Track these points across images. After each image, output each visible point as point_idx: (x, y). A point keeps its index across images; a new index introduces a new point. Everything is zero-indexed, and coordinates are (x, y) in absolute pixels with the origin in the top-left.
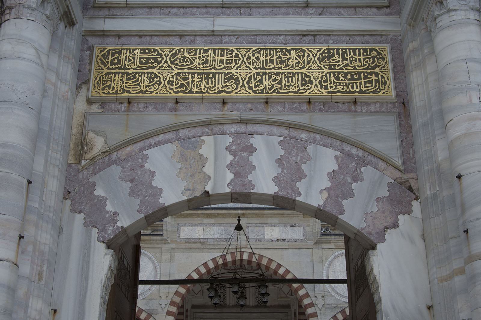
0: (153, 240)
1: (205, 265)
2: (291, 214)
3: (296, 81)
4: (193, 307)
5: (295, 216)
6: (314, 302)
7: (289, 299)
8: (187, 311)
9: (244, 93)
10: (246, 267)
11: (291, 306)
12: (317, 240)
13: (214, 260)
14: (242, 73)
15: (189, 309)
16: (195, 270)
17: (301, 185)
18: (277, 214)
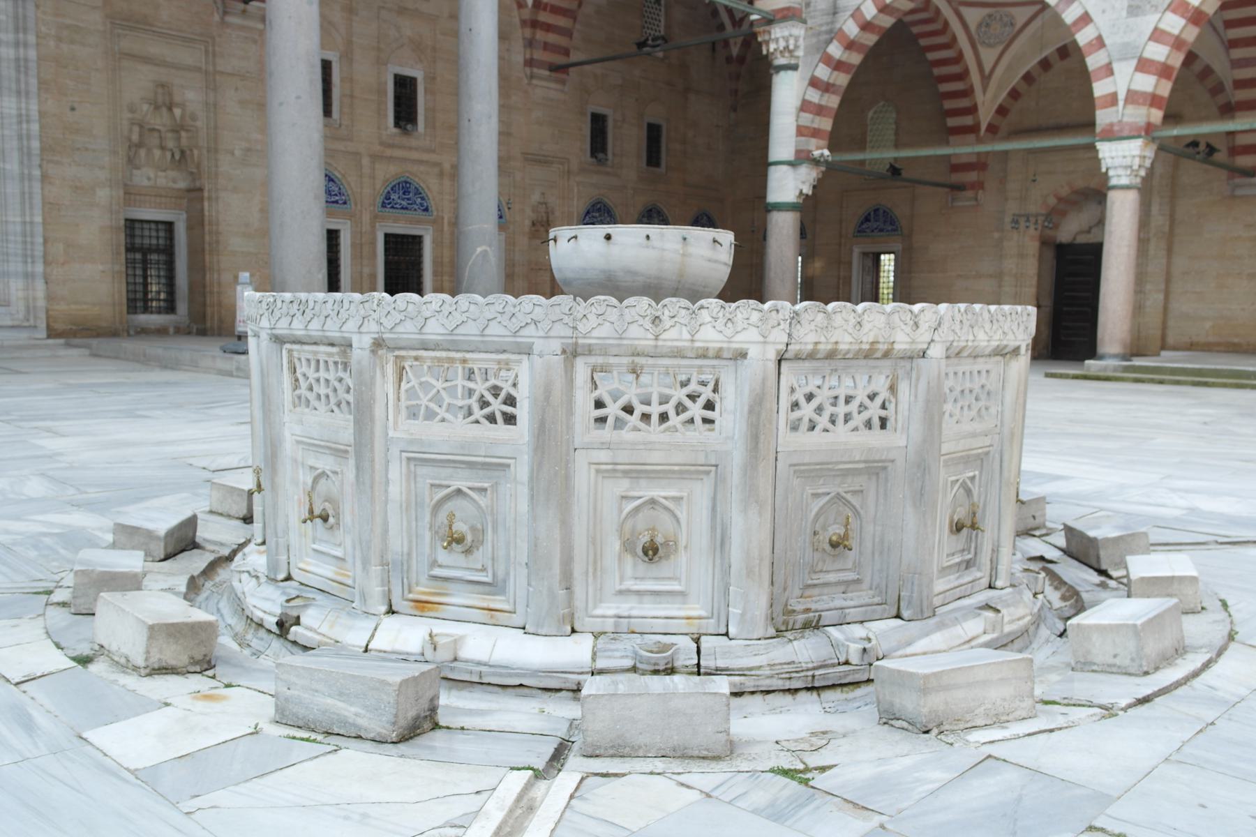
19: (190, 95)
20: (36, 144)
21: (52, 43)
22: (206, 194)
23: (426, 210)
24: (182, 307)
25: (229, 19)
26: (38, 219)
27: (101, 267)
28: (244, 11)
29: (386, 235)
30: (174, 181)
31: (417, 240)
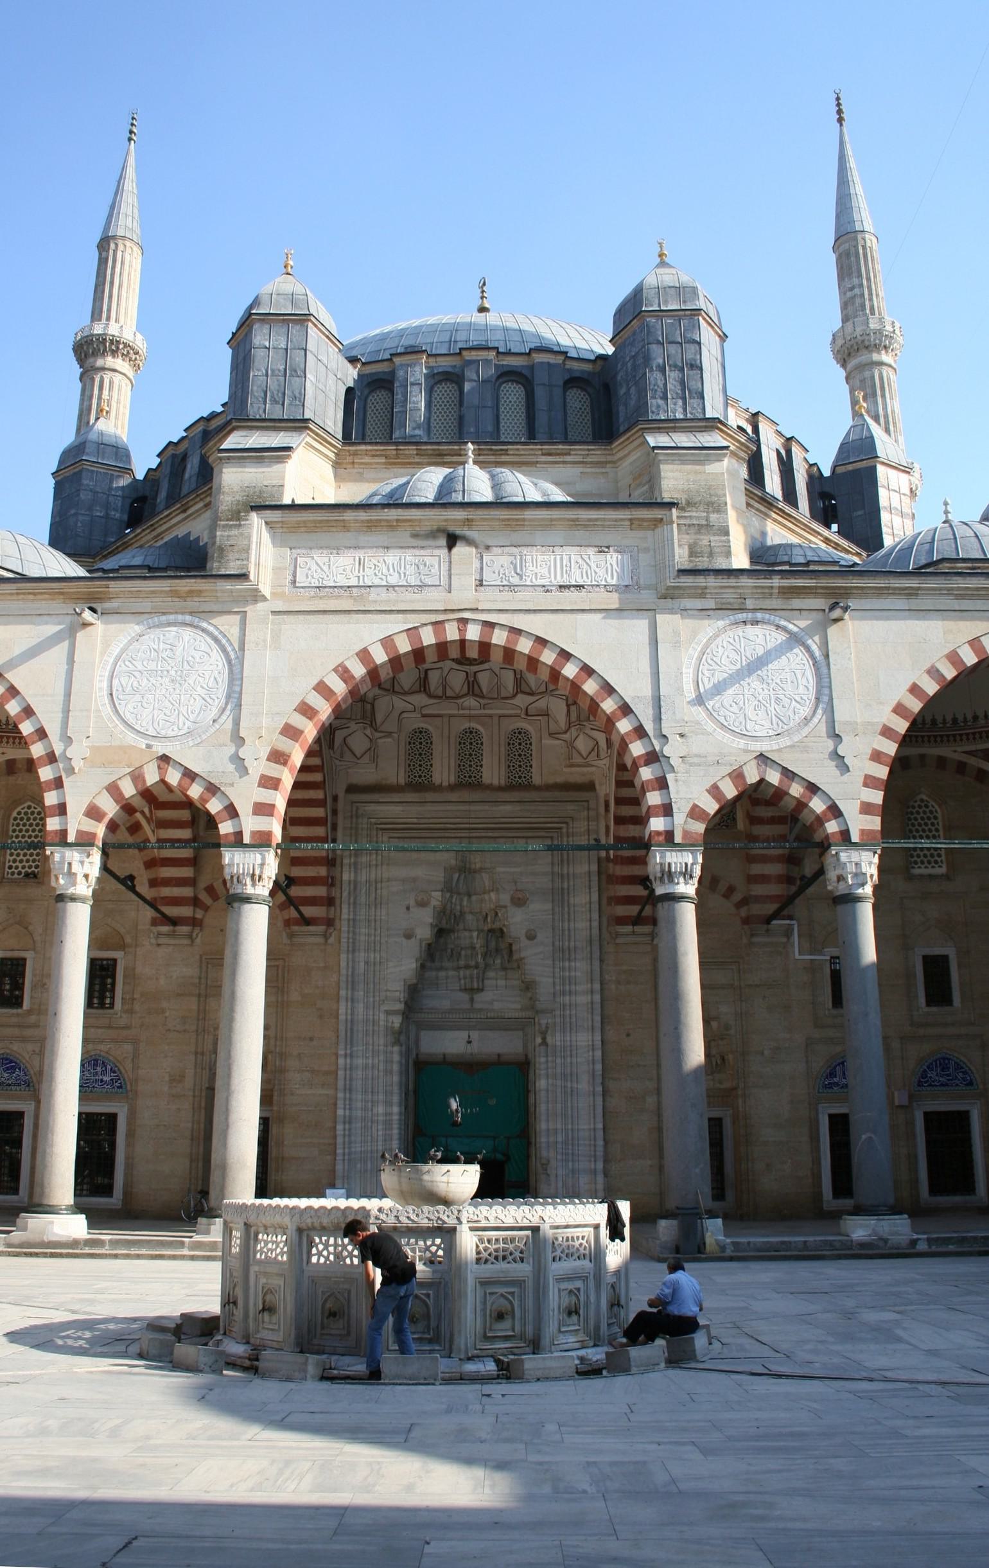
0: (223, 591)
1: (364, 655)
2: (596, 520)
4: (352, 789)
5: (609, 526)
6: (657, 748)
7: (594, 769)
8: (335, 798)
10: (485, 691)
11: (597, 787)
12: (668, 588)
13: (387, 642)
15: (341, 795)
16: (335, 670)
18: (560, 519)
19: (724, 1009)
20: (599, 1067)
21: (613, 986)
22: (740, 1092)
23: (971, 1083)
24: (730, 1194)
25: (755, 940)
26: (600, 1126)
27: (649, 1162)
28: (767, 930)
29: (926, 1114)
30: (721, 1083)
31: (963, 1118)
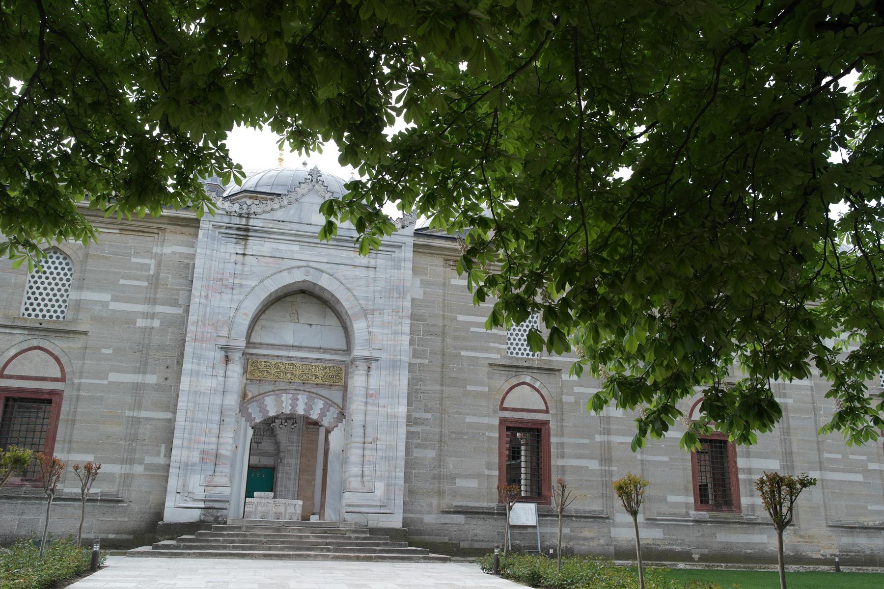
3: (314, 377)
9: (297, 380)
14: (297, 373)
17: (311, 412)
